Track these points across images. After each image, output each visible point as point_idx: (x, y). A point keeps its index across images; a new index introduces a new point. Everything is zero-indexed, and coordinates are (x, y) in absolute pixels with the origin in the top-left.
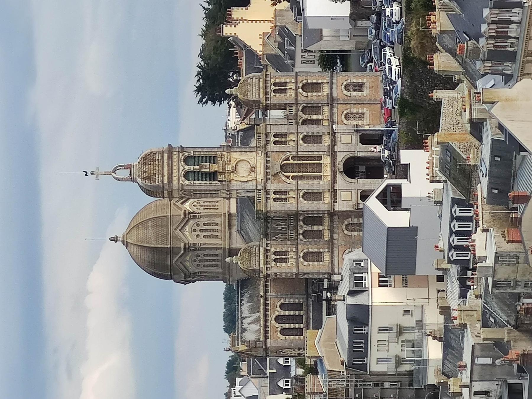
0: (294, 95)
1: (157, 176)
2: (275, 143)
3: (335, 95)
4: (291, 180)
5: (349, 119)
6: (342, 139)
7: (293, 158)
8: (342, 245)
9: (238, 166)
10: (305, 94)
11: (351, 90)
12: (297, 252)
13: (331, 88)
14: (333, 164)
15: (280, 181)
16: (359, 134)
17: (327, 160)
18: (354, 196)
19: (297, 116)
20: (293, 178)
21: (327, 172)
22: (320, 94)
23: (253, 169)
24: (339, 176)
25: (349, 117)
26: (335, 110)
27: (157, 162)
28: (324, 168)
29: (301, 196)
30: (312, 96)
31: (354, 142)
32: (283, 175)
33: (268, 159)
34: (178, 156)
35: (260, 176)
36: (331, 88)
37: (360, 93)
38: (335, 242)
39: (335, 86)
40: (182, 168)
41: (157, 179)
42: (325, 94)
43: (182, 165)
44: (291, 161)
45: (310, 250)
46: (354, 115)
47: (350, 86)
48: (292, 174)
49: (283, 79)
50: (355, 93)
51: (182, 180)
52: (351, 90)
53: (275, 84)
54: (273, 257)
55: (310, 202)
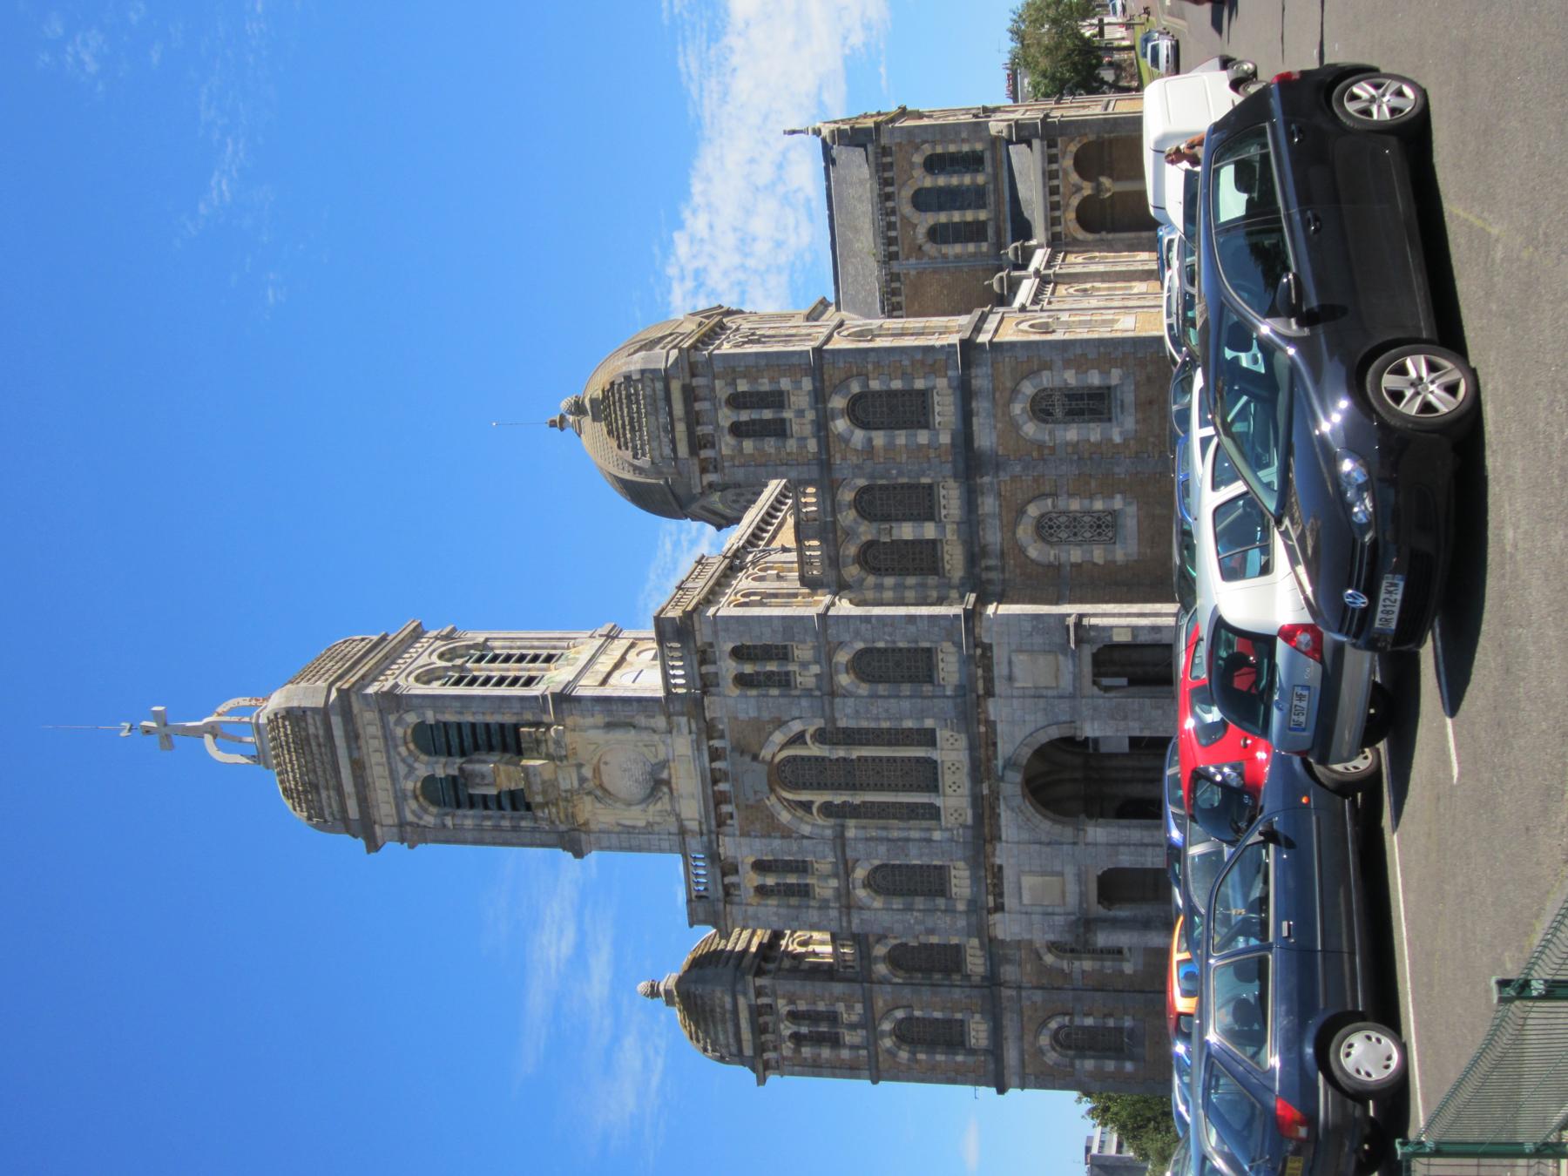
0: (812, 445)
1: (324, 794)
2: (742, 681)
3: (985, 438)
4: (820, 821)
5: (1051, 535)
6: (1017, 672)
7: (821, 737)
8: (1034, 1003)
9: (606, 763)
10: (859, 436)
11: (1058, 412)
12: (869, 1023)
13: (967, 415)
14: (981, 769)
15: (773, 828)
16: (1087, 652)
17: (951, 752)
18: (1072, 888)
19: (835, 532)
20: (827, 809)
21: (954, 800)
22: (923, 437)
23: (658, 784)
24: (1006, 816)
25: (1051, 527)
26: (988, 504)
27: (313, 744)
28: (947, 779)
29: (859, 883)
30: (890, 447)
31: (1066, 683)
32: (787, 800)
33: (716, 743)
34: (384, 726)
35: (692, 810)
36: (967, 415)
37: (1094, 432)
38: (1007, 992)
39: (980, 406)
40: (402, 769)
41: (324, 803)
42: (945, 439)
43: (403, 760)
44: (815, 750)
45: (917, 1013)
46: (1075, 519)
47: (1051, 395)
48: (819, 798)
49: (766, 381)
50: (1072, 434)
51: (413, 812)
52: (1058, 412)
53: (737, 401)
54: (787, 1029)
55: (897, 903)
